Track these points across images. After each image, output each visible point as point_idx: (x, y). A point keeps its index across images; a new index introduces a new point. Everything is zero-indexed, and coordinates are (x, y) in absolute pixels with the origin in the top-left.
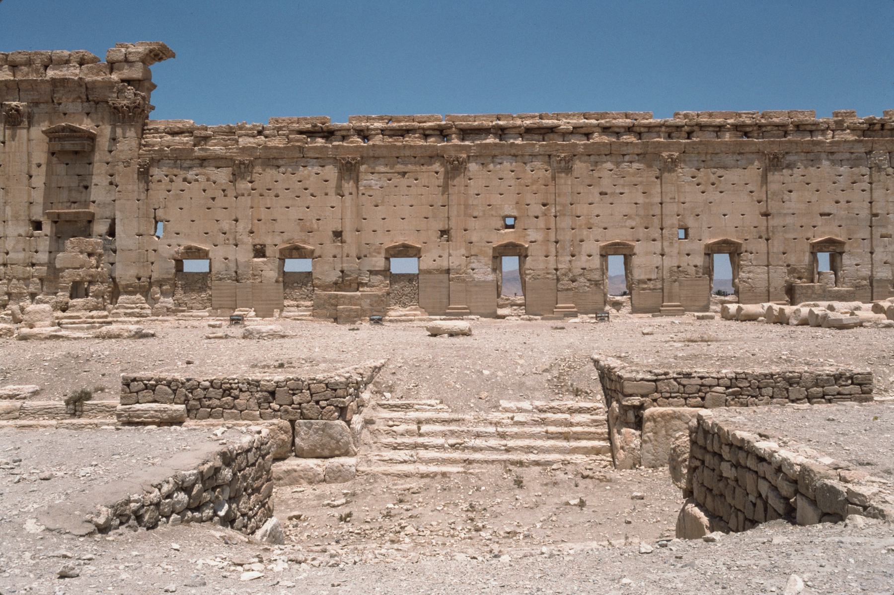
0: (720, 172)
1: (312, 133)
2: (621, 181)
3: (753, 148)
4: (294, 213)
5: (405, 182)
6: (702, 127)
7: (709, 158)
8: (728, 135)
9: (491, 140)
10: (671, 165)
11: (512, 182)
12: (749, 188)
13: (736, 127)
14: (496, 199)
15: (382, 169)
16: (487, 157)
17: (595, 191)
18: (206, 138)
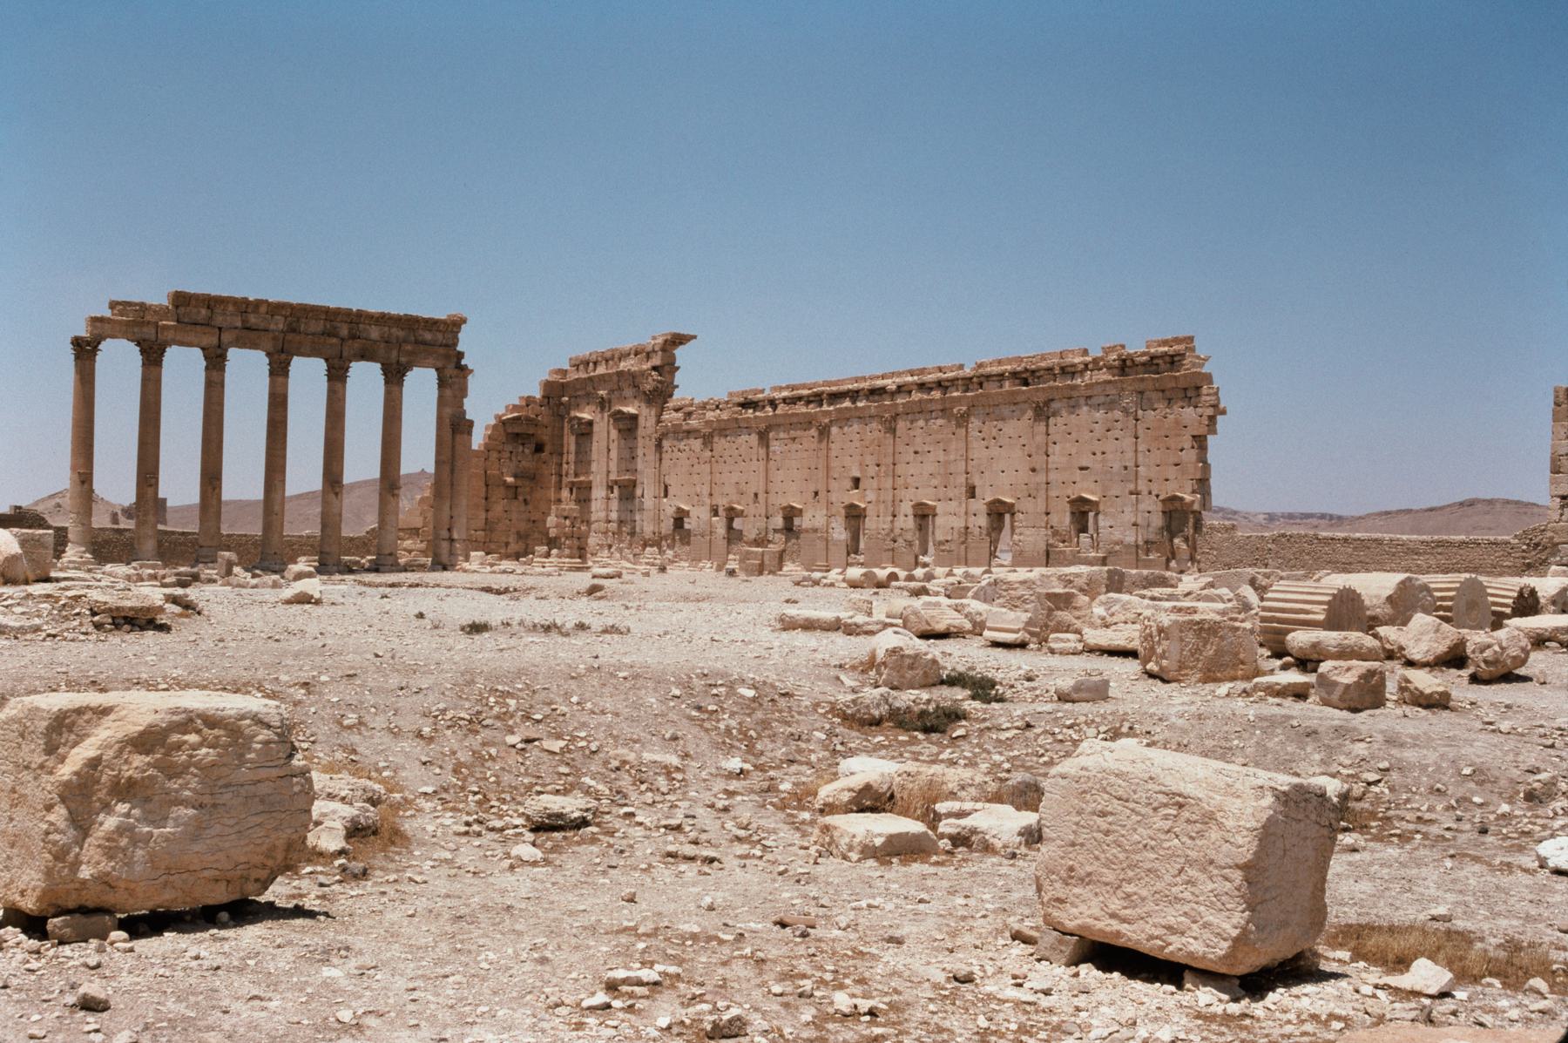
0: (1000, 424)
1: (746, 405)
2: (928, 439)
4: (735, 477)
5: (795, 446)
6: (988, 377)
7: (991, 411)
8: (1007, 384)
9: (847, 404)
11: (858, 444)
12: (1022, 441)
13: (1014, 374)
14: (847, 461)
15: (782, 435)
16: (844, 419)
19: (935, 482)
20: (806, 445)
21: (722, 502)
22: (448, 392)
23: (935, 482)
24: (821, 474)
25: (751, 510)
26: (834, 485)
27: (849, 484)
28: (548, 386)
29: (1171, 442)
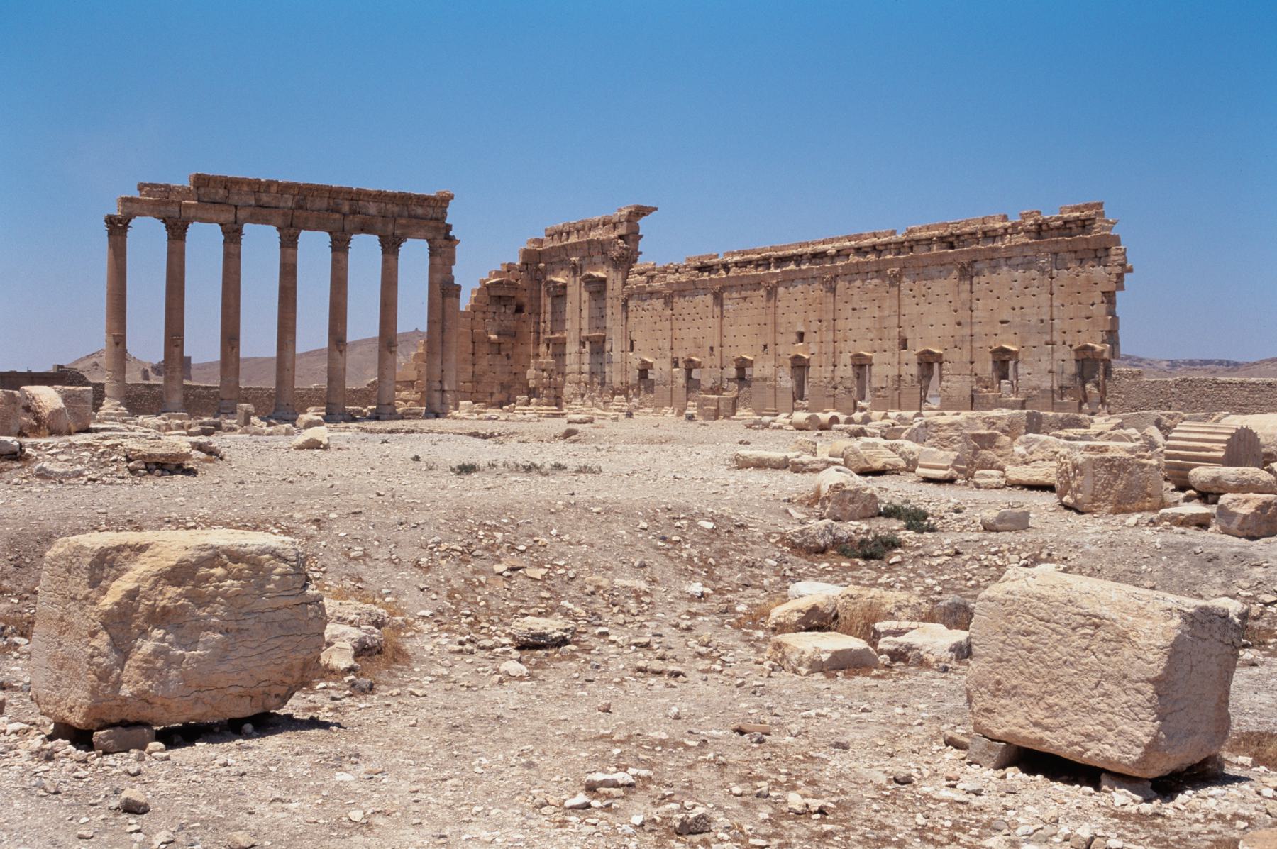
0: (929, 283)
1: (702, 268)
2: (865, 297)
3: (950, 259)
4: (693, 333)
5: (745, 305)
6: (918, 241)
7: (922, 271)
8: (935, 247)
9: (792, 266)
10: (895, 280)
11: (802, 302)
12: (949, 298)
13: (941, 239)
14: (793, 317)
15: (735, 295)
16: (789, 280)
17: (850, 306)
18: (652, 277)
19: (870, 335)
20: (755, 304)
21: (682, 355)
22: (438, 260)
23: (870, 335)
24: (770, 328)
25: (707, 362)
26: (781, 339)
27: (794, 338)
28: (527, 254)
29: (1083, 298)
